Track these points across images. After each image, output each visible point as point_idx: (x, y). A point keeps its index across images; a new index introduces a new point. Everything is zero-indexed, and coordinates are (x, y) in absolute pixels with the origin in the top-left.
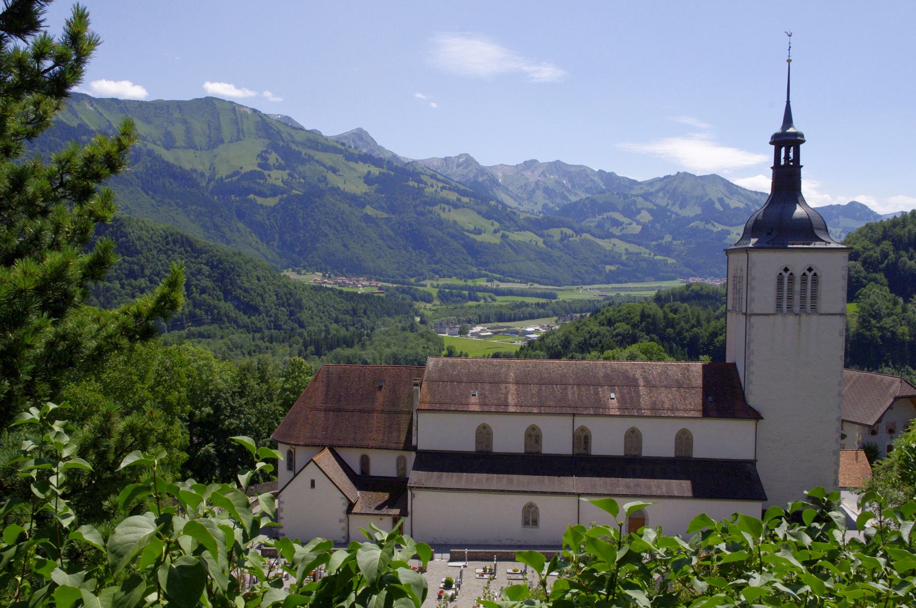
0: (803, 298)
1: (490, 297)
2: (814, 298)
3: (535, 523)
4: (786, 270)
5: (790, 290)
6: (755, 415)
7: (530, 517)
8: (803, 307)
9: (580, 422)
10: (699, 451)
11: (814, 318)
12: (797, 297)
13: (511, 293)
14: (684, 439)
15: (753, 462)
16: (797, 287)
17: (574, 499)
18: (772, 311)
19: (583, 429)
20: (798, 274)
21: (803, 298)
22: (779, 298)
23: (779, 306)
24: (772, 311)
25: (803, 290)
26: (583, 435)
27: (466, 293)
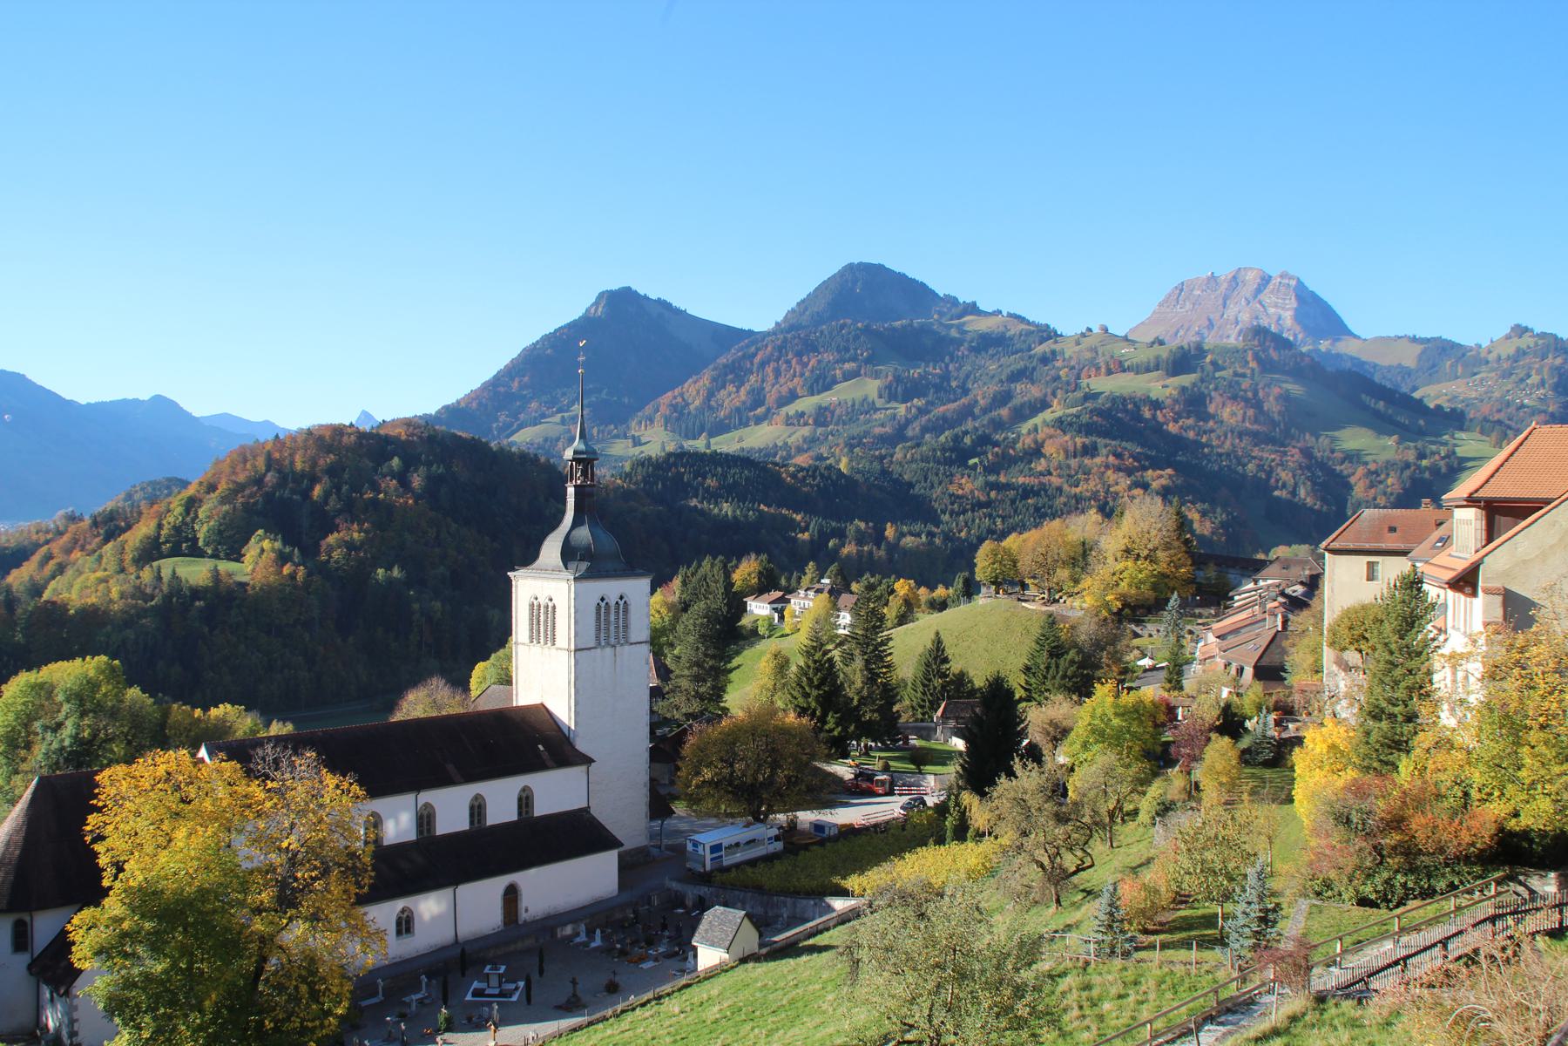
2: (626, 627)
5: (607, 621)
6: (587, 761)
7: (405, 924)
8: (617, 637)
9: (427, 796)
10: (541, 809)
11: (627, 647)
12: (612, 628)
14: (525, 801)
15: (586, 810)
16: (612, 617)
18: (592, 644)
19: (427, 805)
20: (612, 604)
22: (598, 629)
23: (598, 638)
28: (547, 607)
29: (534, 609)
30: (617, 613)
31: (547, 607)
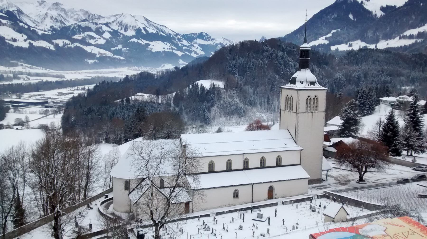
0: (313, 106)
1: (27, 77)
2: (316, 106)
3: (237, 196)
4: (309, 97)
8: (313, 109)
11: (317, 113)
12: (312, 106)
13: (37, 75)
16: (312, 103)
17: (251, 185)
18: (304, 111)
19: (246, 159)
20: (312, 98)
21: (313, 106)
22: (307, 107)
23: (306, 109)
24: (304, 111)
25: (314, 104)
26: (246, 161)
27: (12, 75)
28: (290, 98)
29: (287, 99)
30: (314, 101)
31: (290, 98)
